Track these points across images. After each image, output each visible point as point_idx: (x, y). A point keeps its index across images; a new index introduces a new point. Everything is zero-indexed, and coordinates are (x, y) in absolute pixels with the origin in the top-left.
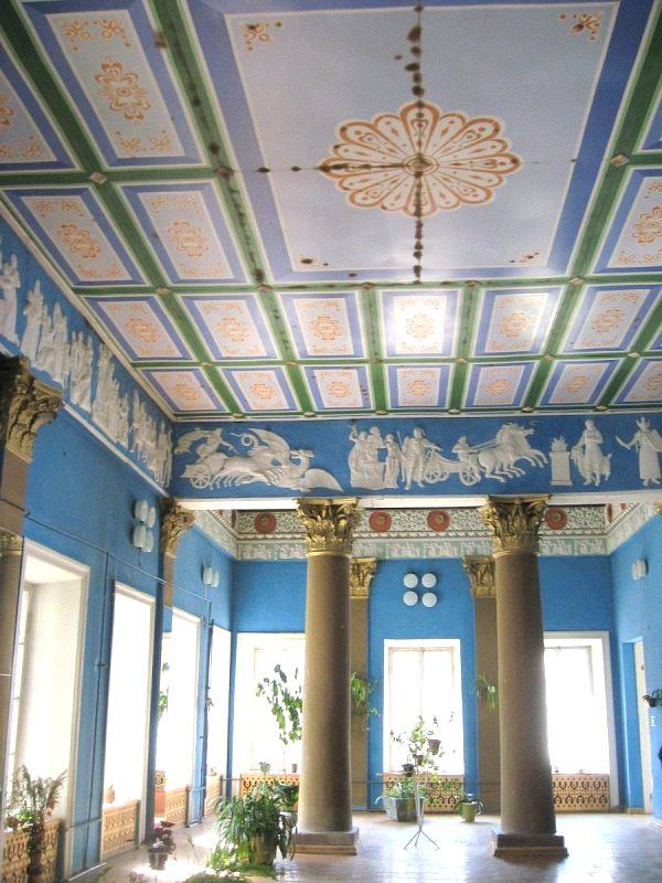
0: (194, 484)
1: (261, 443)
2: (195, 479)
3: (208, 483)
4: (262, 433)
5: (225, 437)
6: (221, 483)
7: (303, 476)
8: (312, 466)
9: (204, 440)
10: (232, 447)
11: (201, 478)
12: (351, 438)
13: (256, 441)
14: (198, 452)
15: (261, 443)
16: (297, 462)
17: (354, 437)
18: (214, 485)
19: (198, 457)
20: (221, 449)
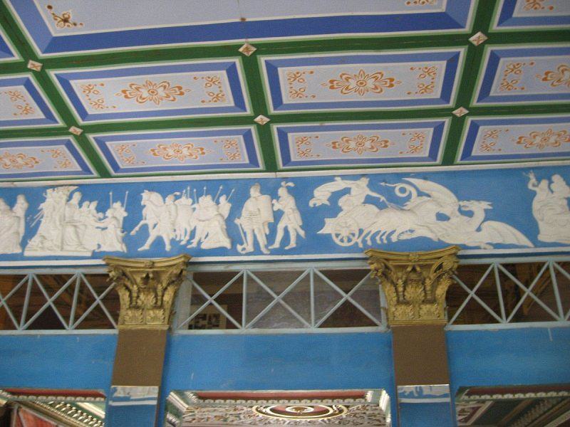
0: (337, 241)
1: (420, 194)
2: (337, 235)
3: (354, 240)
4: (419, 182)
5: (371, 186)
6: (373, 239)
7: (479, 230)
8: (489, 216)
9: (346, 191)
10: (383, 199)
11: (344, 233)
12: (530, 187)
13: (414, 193)
14: (340, 204)
15: (420, 194)
16: (470, 214)
17: (534, 185)
18: (364, 241)
19: (340, 210)
20: (369, 200)
